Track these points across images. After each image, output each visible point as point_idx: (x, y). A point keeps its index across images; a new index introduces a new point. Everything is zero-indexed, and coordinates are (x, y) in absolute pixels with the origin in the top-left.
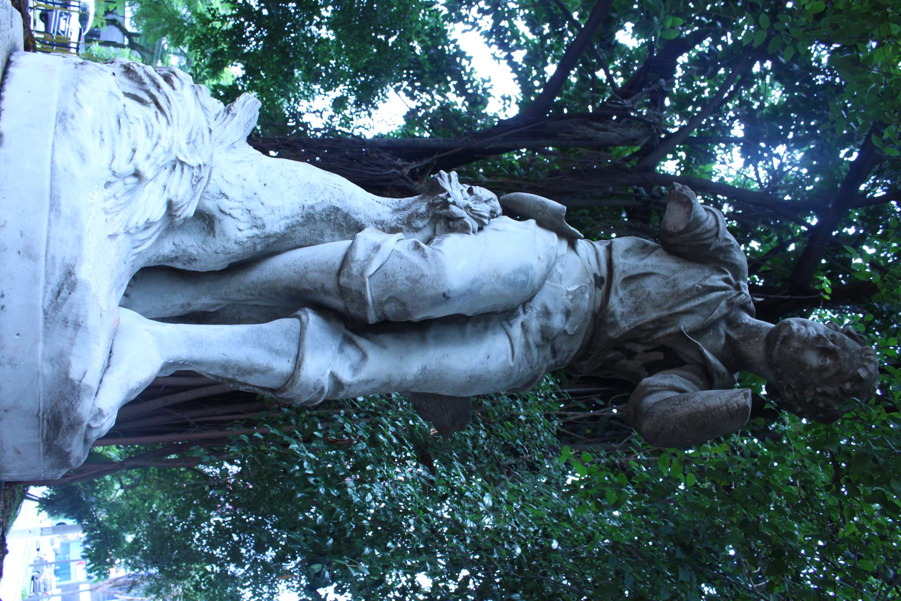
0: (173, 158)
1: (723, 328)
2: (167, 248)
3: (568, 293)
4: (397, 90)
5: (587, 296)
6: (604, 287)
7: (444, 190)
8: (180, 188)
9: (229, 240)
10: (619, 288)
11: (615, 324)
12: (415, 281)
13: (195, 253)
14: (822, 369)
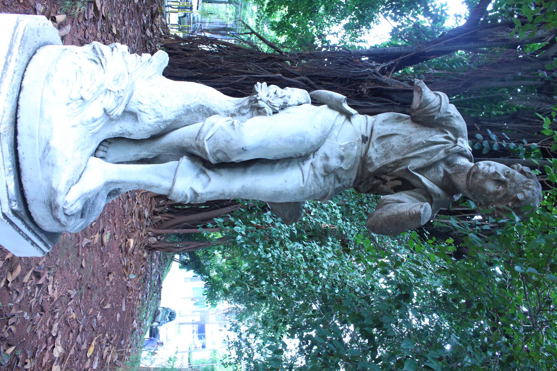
0: (105, 89)
1: (442, 167)
2: (116, 129)
3: (340, 146)
4: (385, 16)
5: (356, 148)
6: (367, 142)
7: (257, 93)
8: (109, 102)
9: (145, 124)
10: (375, 143)
11: (372, 164)
12: (228, 142)
13: (131, 131)
14: (497, 193)
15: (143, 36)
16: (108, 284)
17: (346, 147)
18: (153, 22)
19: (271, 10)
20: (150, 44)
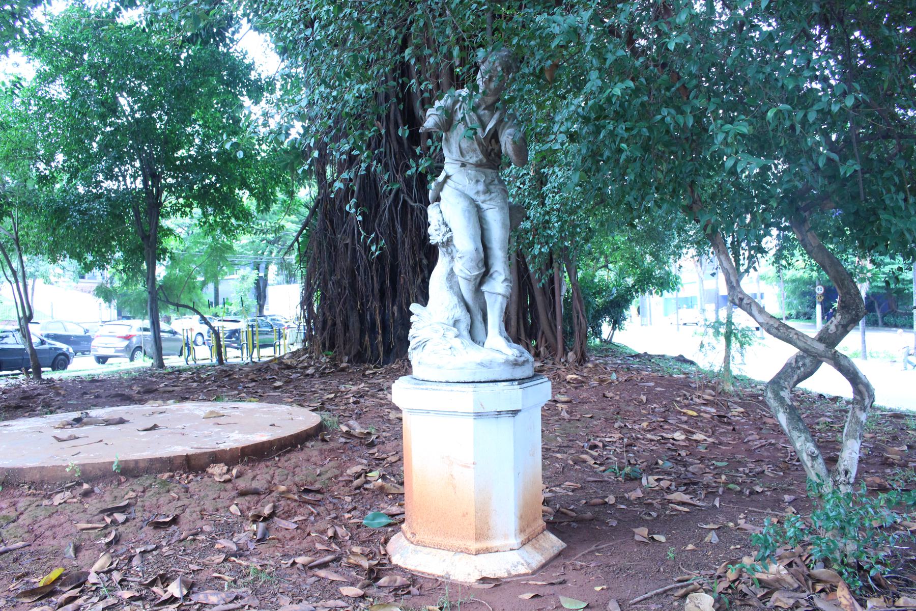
2: (465, 333)
4: (232, 41)
11: (481, 160)
15: (317, 375)
16: (617, 398)
17: (470, 179)
18: (295, 368)
19: (245, 215)
20: (324, 369)
